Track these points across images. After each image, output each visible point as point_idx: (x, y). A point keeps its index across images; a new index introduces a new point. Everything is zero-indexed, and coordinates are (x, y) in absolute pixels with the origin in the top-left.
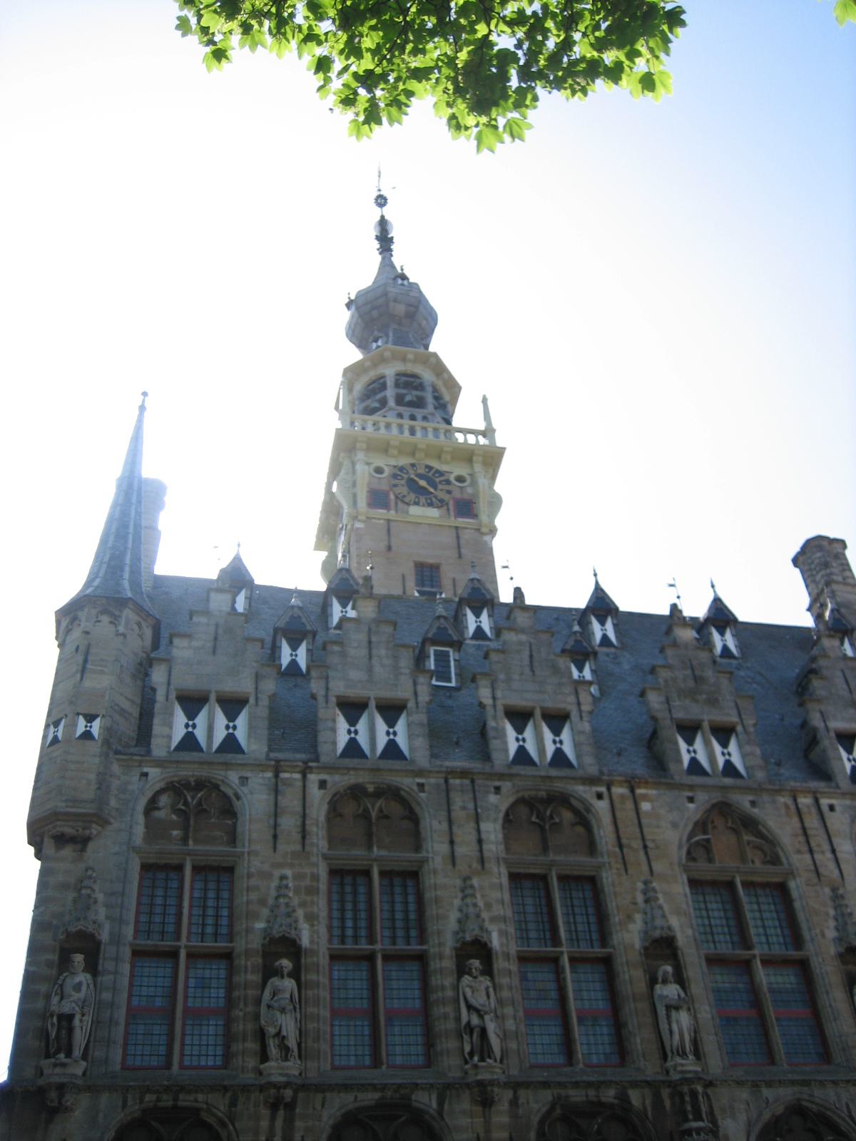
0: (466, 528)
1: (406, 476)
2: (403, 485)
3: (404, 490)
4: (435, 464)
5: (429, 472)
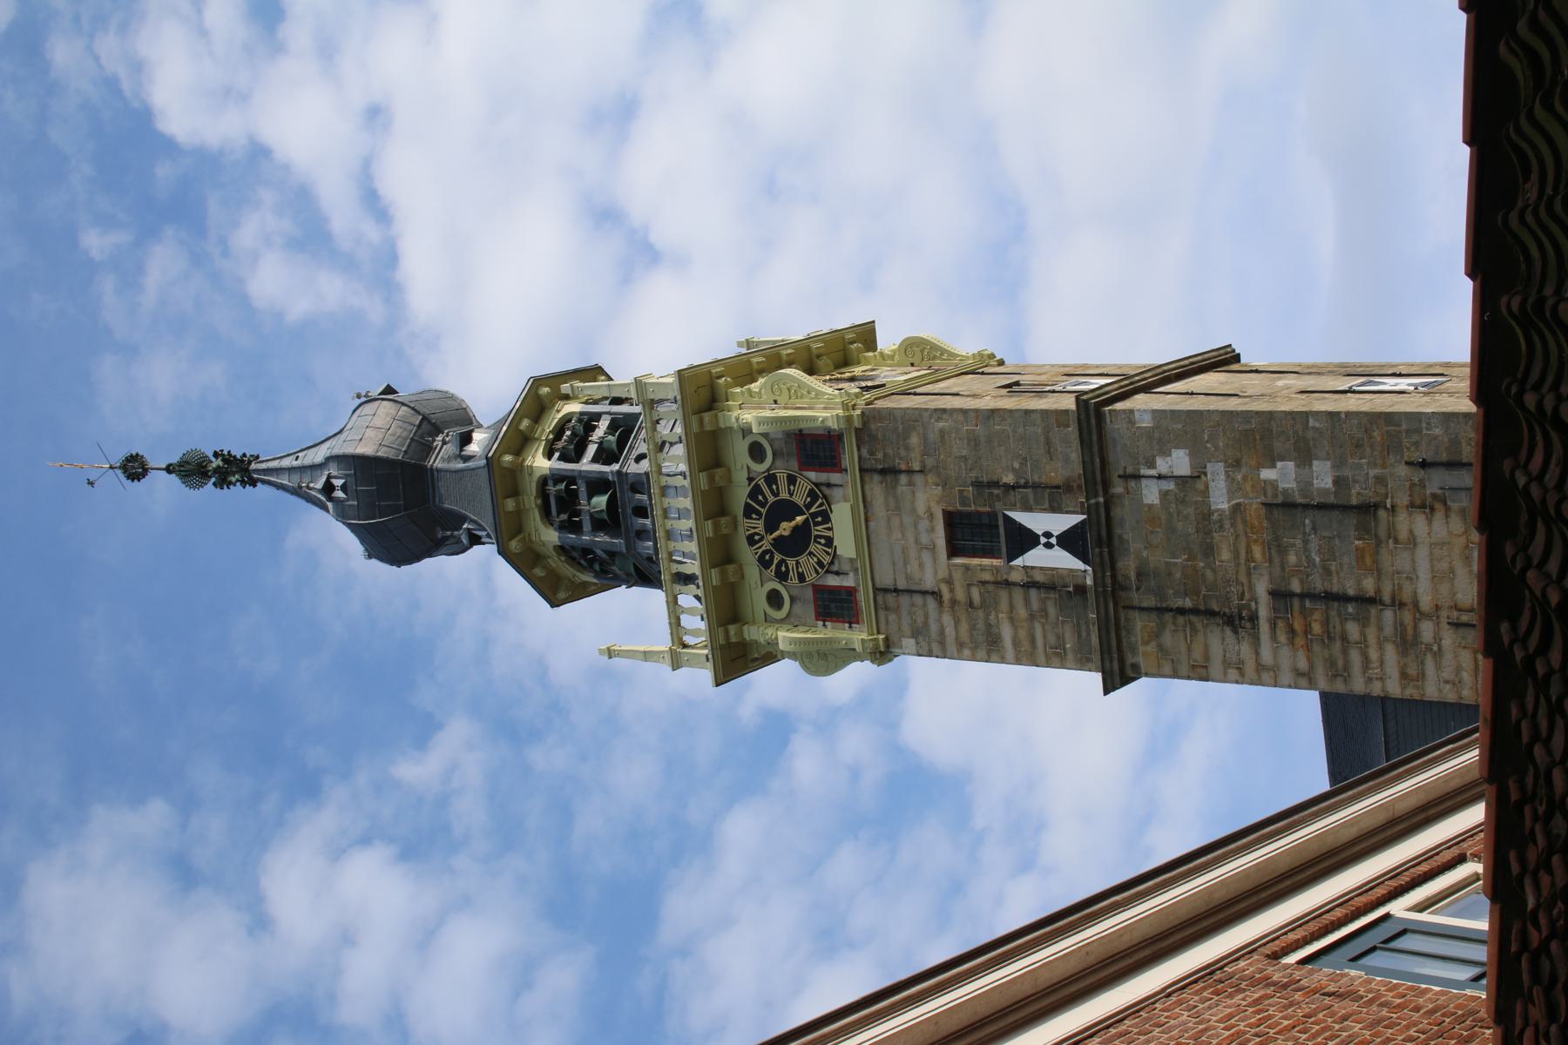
0: (860, 457)
1: (777, 557)
2: (798, 563)
3: (807, 563)
4: (741, 495)
5: (759, 514)
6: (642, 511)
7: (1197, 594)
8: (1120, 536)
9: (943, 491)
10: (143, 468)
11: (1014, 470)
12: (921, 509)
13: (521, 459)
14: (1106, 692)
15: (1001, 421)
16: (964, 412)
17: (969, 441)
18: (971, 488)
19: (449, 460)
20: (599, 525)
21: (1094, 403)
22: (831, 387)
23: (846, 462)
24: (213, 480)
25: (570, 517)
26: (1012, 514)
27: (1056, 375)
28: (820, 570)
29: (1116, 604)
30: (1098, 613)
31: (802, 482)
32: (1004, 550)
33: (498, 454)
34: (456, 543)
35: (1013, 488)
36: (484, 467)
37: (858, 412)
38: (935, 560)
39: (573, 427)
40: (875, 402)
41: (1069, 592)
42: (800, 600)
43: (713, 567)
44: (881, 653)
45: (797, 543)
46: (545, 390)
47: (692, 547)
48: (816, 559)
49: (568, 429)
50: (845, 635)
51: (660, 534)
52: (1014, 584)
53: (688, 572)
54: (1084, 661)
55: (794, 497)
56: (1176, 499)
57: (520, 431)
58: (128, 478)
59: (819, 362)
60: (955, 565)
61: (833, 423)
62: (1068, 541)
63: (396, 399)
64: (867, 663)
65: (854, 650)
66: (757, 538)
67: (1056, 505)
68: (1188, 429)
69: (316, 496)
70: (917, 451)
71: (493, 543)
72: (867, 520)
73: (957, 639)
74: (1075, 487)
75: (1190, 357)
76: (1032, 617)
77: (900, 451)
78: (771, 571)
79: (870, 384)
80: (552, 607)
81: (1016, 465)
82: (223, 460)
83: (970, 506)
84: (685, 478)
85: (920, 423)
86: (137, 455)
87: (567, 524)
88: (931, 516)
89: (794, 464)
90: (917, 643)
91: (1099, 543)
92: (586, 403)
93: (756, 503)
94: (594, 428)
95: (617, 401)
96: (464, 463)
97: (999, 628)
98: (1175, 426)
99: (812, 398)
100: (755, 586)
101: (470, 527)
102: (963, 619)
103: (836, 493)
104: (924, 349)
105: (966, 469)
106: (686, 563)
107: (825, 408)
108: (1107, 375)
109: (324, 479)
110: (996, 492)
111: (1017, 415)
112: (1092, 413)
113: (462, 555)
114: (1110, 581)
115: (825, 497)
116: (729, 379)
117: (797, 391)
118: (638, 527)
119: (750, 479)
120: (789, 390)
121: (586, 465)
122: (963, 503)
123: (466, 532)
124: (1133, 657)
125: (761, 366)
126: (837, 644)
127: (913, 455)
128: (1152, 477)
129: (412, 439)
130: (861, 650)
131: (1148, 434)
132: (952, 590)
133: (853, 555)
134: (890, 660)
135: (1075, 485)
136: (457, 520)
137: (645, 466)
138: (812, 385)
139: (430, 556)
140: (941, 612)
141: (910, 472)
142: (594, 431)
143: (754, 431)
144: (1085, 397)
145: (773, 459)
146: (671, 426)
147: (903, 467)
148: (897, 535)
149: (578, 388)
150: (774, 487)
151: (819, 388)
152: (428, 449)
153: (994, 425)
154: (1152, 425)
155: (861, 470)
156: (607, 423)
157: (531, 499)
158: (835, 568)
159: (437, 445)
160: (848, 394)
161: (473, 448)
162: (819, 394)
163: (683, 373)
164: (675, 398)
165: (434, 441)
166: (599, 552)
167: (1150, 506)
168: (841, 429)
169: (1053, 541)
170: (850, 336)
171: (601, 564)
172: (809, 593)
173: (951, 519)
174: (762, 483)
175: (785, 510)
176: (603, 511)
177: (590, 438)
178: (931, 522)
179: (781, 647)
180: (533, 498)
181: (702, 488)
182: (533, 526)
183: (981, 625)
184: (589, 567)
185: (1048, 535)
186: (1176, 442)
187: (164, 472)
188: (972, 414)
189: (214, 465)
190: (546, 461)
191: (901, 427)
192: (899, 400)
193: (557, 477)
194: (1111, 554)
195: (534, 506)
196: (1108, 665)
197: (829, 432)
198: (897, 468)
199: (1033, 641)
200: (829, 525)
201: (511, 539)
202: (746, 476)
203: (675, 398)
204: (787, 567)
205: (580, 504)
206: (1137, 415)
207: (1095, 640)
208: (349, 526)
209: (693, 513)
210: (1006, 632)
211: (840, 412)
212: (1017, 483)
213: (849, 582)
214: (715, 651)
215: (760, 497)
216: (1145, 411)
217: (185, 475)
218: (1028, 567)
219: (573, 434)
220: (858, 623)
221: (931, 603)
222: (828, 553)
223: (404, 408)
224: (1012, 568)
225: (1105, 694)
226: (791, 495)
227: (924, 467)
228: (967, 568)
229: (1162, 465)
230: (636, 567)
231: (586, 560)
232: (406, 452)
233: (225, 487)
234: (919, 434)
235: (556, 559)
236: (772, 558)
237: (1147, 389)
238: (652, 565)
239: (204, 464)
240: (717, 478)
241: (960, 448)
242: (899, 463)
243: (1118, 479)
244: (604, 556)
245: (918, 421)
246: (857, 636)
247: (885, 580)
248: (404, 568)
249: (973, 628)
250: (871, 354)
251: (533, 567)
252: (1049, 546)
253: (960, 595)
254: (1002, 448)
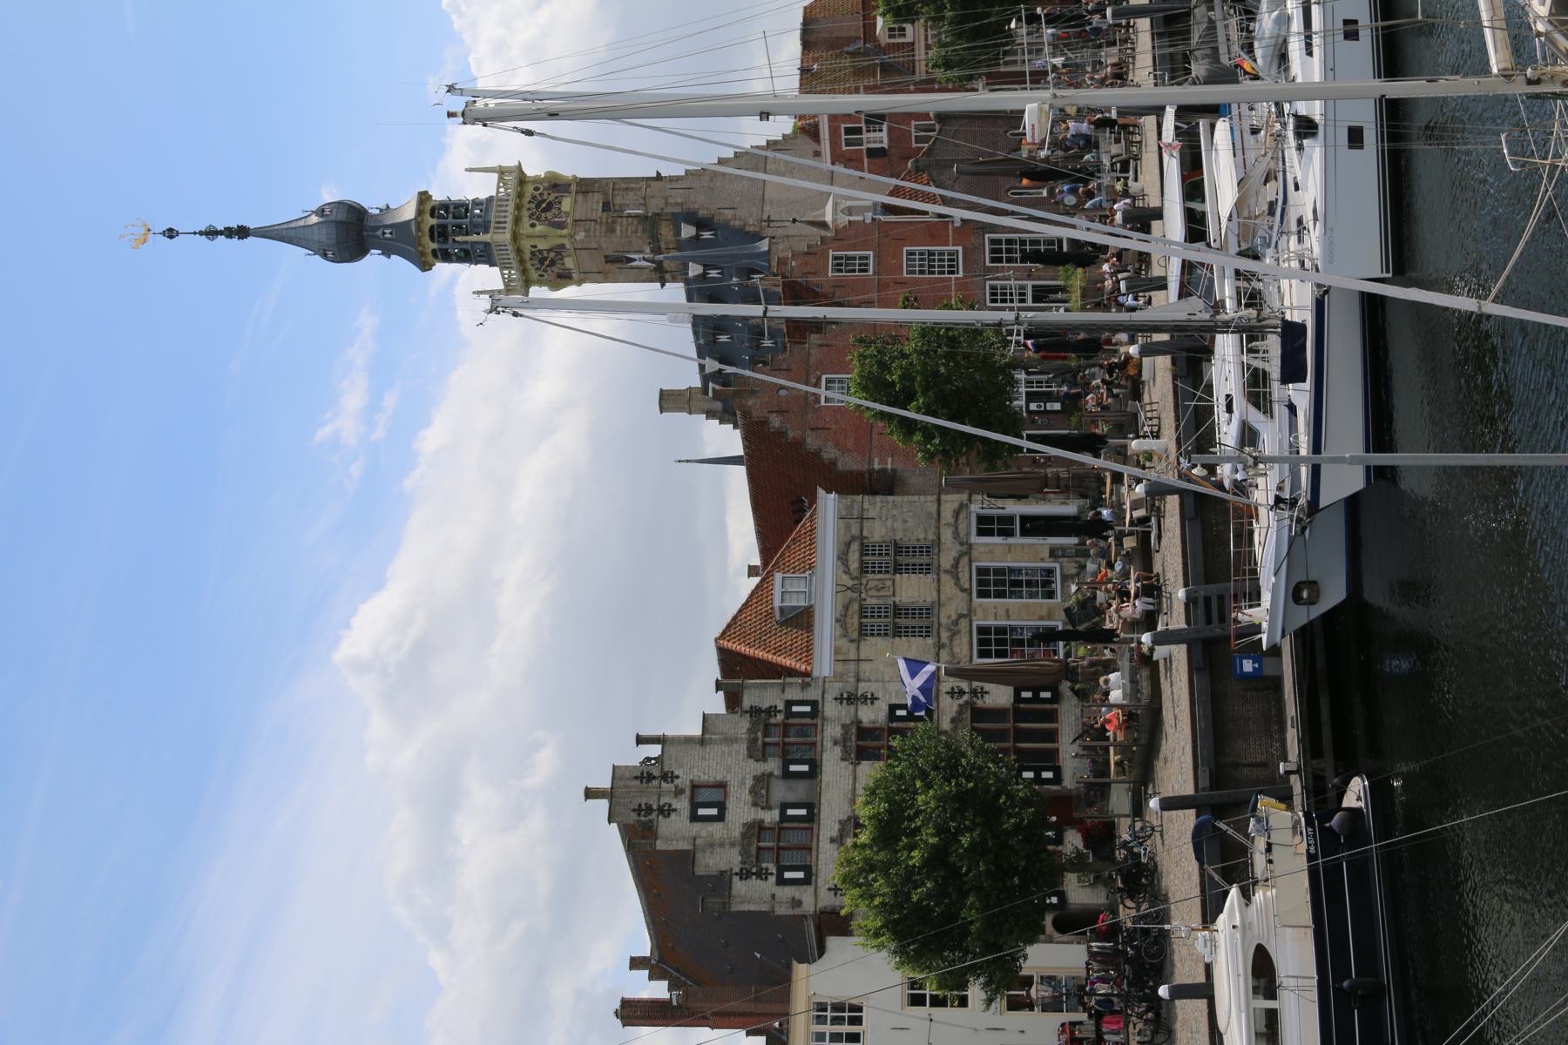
3: (549, 215)
12: (595, 199)
45: (549, 207)
88: (598, 202)
213: (564, 219)
247: (578, 217)
253: (604, 220)
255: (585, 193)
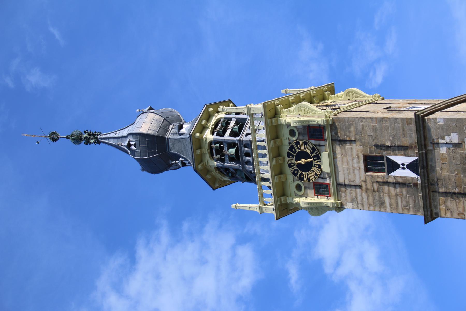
0: (331, 135)
2: (307, 174)
3: (311, 174)
4: (286, 149)
5: (293, 156)
6: (248, 155)
7: (461, 187)
8: (431, 165)
9: (363, 148)
10: (57, 137)
11: (390, 140)
13: (202, 135)
14: (425, 223)
15: (386, 122)
16: (372, 119)
17: (373, 130)
18: (374, 147)
19: (174, 134)
20: (231, 159)
21: (422, 115)
22: (319, 109)
23: (326, 137)
24: (84, 141)
25: (221, 156)
26: (389, 157)
27: (405, 104)
28: (316, 177)
29: (429, 190)
30: (422, 194)
31: (310, 144)
32: (386, 170)
33: (194, 134)
34: (176, 165)
35: (390, 147)
36: (188, 138)
37: (331, 118)
38: (360, 173)
39: (222, 123)
40: (337, 114)
41: (412, 186)
42: (308, 188)
43: (276, 175)
44: (339, 207)
45: (308, 167)
46: (211, 109)
47: (268, 168)
48: (314, 173)
49: (220, 124)
50: (325, 201)
51: (255, 163)
52: (390, 183)
53: (266, 177)
54: (417, 211)
55: (306, 150)
56: (453, 151)
57: (202, 125)
58: (52, 140)
59: (313, 98)
60: (368, 175)
61: (322, 123)
62: (411, 167)
63: (154, 112)
64: (334, 212)
65: (329, 206)
66: (292, 165)
67: (406, 153)
68: (457, 125)
69: (123, 148)
70: (353, 133)
71: (192, 166)
72: (334, 159)
73: (368, 202)
74: (414, 147)
75: (456, 97)
76: (397, 195)
77: (347, 133)
78: (297, 177)
79: (334, 107)
80: (213, 189)
81: (391, 138)
82: (88, 134)
83: (373, 153)
84: (265, 143)
85: (354, 123)
86: (55, 132)
87: (219, 159)
88: (358, 157)
89: (307, 138)
90: (353, 204)
91: (423, 168)
92: (226, 114)
93: (292, 152)
94: (229, 124)
95: (237, 114)
96: (180, 136)
97: (384, 199)
98: (452, 124)
99: (313, 113)
100: (291, 183)
101: (183, 159)
102: (370, 195)
103: (323, 148)
104: (354, 94)
105: (372, 140)
106: (265, 174)
107: (318, 117)
108: (424, 104)
109: (127, 142)
110: (383, 148)
111: (391, 120)
112: (421, 119)
113: (178, 169)
114: (427, 182)
115: (318, 150)
116: (281, 106)
117: (307, 111)
118: (246, 160)
119: (290, 143)
120: (305, 110)
121: (227, 137)
122: (371, 153)
123: (181, 162)
124: (436, 210)
125: (293, 101)
126: (322, 204)
127: (351, 134)
128: (444, 143)
129: (160, 127)
130: (332, 207)
131: (442, 127)
132: (366, 185)
133: (329, 171)
134: (342, 210)
135: (414, 146)
136: (177, 157)
137: (249, 137)
138: (313, 108)
139: (167, 170)
140: (362, 193)
141: (351, 141)
142: (229, 124)
143: (292, 125)
144: (418, 113)
145: (298, 136)
146: (261, 125)
147: (348, 139)
148: (345, 164)
149: (225, 109)
150: (299, 146)
151: (316, 110)
152: (166, 131)
153: (383, 124)
154: (443, 124)
155: (332, 140)
156: (234, 121)
157: (206, 150)
158: (322, 176)
159: (169, 130)
160: (327, 112)
161: (183, 131)
162: (316, 112)
163: (265, 104)
164: (262, 113)
165: (168, 128)
166: (231, 169)
167: (443, 154)
168: (325, 125)
169: (405, 167)
170: (325, 89)
171: (232, 174)
172: (312, 185)
173: (366, 158)
174: (294, 145)
175: (305, 155)
176: (233, 154)
177: (228, 127)
178: (358, 159)
179: (301, 205)
180: (207, 150)
181: (272, 146)
182: (207, 160)
183: (377, 198)
184: (227, 175)
185: (403, 164)
186: (453, 130)
187: (66, 138)
188: (375, 119)
189: (85, 136)
190: (212, 135)
191: (347, 124)
192: (346, 114)
193: (216, 142)
194: (427, 171)
195: (207, 152)
196: (426, 213)
197: (320, 126)
198: (346, 139)
199: (397, 204)
200: (320, 160)
201: (199, 164)
202: (288, 142)
203: (262, 113)
204: (303, 175)
205: (224, 152)
206: (438, 120)
207: (421, 203)
208: (137, 159)
209: (268, 156)
210: (387, 200)
211: (324, 119)
212: (391, 145)
213: (328, 181)
214: (276, 207)
215: (293, 150)
216: (441, 119)
217: (73, 140)
218: (395, 176)
219: (221, 125)
220: (330, 196)
221: (358, 190)
222: (319, 171)
223: (157, 116)
224: (389, 177)
225: (425, 223)
226: (305, 149)
227: (356, 139)
228: (372, 176)
229: (447, 139)
230: (245, 175)
231: (226, 173)
232: (158, 132)
233: (89, 144)
234: (354, 127)
235: (215, 172)
236: (298, 172)
237: (440, 110)
238: (252, 174)
239: (81, 136)
240: (277, 143)
241: (370, 132)
242: (346, 138)
243: (431, 144)
244: (233, 171)
245: (353, 122)
246: (330, 201)
247: (341, 181)
248: (156, 175)
249: (374, 199)
250: (333, 96)
251: (206, 175)
252: (403, 168)
253: (369, 186)
254: (386, 132)
255: (343, 142)
